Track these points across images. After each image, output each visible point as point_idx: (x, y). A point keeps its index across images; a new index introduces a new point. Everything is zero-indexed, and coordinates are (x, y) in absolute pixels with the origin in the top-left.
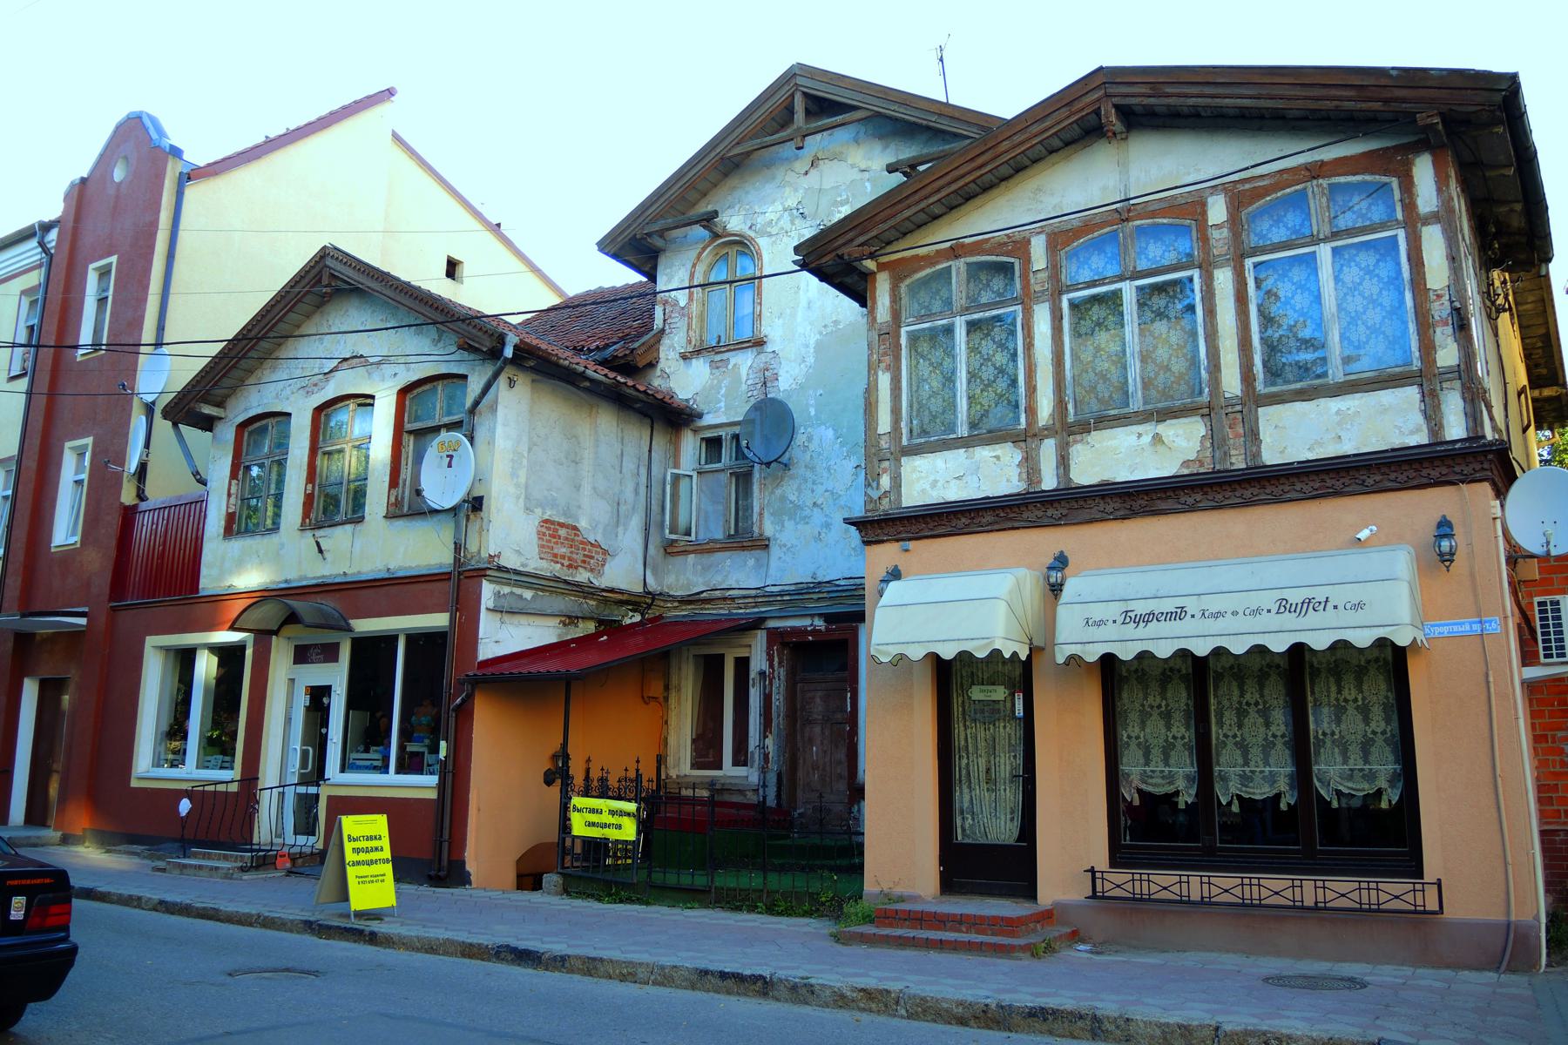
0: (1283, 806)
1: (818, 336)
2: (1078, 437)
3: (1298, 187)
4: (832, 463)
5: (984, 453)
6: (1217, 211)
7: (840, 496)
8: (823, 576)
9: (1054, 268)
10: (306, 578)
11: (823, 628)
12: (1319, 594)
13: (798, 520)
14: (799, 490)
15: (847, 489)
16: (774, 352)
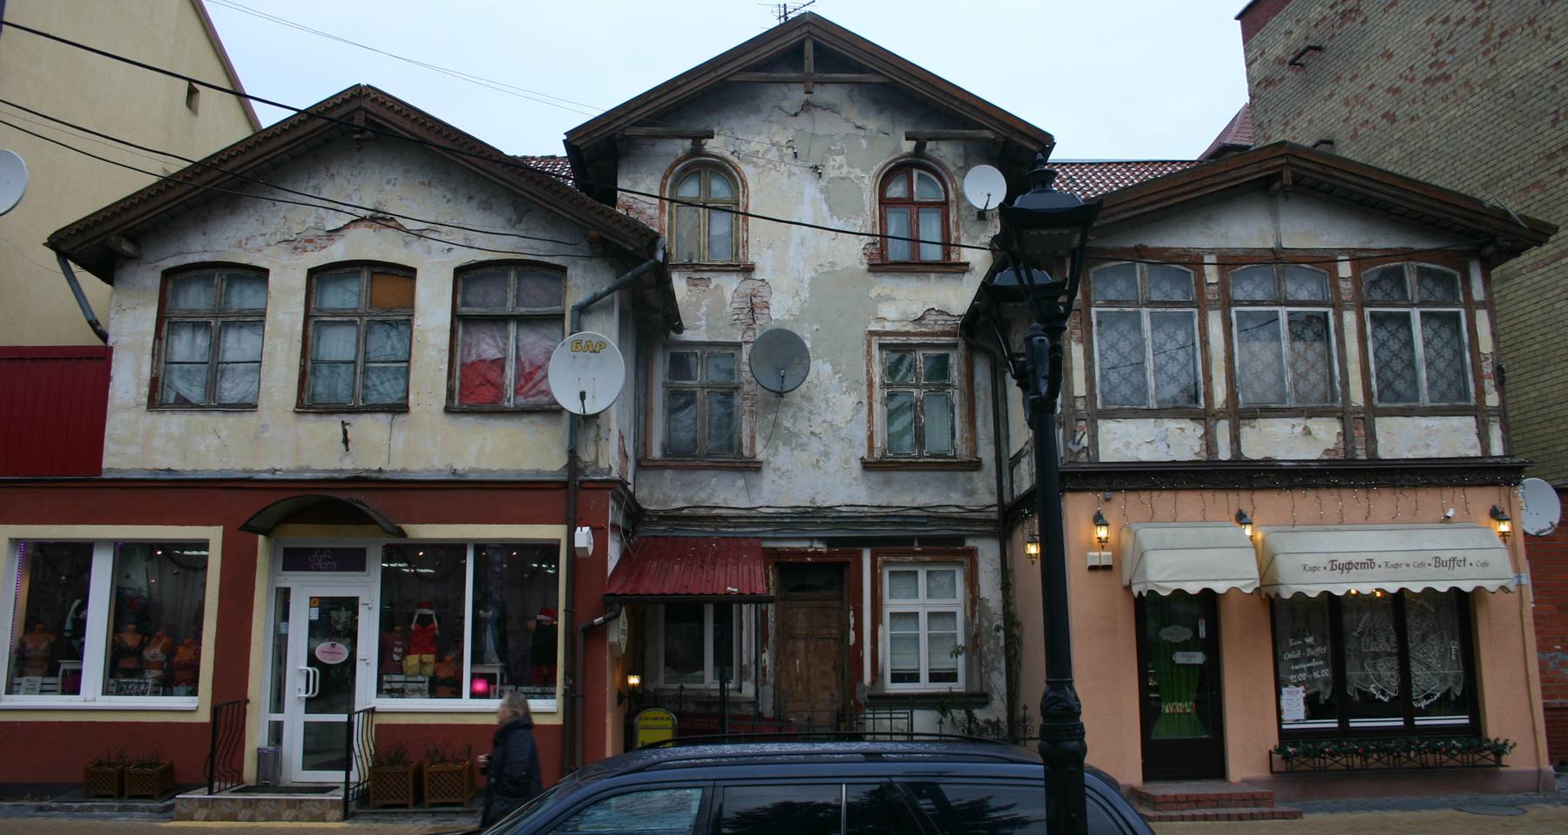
0: (1453, 697)
1: (813, 274)
2: (1246, 422)
3: (1398, 264)
4: (830, 396)
5: (1172, 425)
6: (1345, 269)
7: (840, 428)
8: (823, 500)
9: (1224, 285)
10: (309, 470)
11: (825, 550)
12: (1460, 555)
13: (793, 446)
14: (794, 417)
15: (847, 422)
16: (763, 280)
